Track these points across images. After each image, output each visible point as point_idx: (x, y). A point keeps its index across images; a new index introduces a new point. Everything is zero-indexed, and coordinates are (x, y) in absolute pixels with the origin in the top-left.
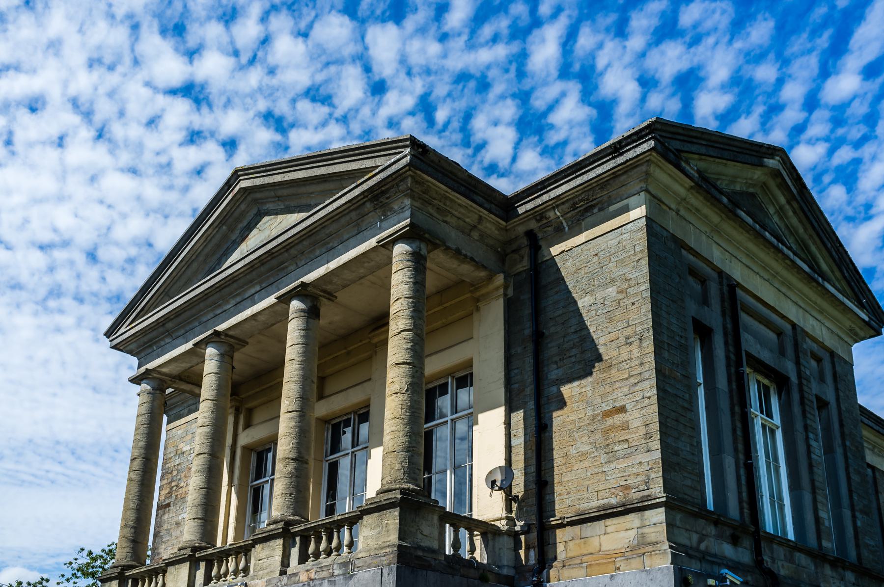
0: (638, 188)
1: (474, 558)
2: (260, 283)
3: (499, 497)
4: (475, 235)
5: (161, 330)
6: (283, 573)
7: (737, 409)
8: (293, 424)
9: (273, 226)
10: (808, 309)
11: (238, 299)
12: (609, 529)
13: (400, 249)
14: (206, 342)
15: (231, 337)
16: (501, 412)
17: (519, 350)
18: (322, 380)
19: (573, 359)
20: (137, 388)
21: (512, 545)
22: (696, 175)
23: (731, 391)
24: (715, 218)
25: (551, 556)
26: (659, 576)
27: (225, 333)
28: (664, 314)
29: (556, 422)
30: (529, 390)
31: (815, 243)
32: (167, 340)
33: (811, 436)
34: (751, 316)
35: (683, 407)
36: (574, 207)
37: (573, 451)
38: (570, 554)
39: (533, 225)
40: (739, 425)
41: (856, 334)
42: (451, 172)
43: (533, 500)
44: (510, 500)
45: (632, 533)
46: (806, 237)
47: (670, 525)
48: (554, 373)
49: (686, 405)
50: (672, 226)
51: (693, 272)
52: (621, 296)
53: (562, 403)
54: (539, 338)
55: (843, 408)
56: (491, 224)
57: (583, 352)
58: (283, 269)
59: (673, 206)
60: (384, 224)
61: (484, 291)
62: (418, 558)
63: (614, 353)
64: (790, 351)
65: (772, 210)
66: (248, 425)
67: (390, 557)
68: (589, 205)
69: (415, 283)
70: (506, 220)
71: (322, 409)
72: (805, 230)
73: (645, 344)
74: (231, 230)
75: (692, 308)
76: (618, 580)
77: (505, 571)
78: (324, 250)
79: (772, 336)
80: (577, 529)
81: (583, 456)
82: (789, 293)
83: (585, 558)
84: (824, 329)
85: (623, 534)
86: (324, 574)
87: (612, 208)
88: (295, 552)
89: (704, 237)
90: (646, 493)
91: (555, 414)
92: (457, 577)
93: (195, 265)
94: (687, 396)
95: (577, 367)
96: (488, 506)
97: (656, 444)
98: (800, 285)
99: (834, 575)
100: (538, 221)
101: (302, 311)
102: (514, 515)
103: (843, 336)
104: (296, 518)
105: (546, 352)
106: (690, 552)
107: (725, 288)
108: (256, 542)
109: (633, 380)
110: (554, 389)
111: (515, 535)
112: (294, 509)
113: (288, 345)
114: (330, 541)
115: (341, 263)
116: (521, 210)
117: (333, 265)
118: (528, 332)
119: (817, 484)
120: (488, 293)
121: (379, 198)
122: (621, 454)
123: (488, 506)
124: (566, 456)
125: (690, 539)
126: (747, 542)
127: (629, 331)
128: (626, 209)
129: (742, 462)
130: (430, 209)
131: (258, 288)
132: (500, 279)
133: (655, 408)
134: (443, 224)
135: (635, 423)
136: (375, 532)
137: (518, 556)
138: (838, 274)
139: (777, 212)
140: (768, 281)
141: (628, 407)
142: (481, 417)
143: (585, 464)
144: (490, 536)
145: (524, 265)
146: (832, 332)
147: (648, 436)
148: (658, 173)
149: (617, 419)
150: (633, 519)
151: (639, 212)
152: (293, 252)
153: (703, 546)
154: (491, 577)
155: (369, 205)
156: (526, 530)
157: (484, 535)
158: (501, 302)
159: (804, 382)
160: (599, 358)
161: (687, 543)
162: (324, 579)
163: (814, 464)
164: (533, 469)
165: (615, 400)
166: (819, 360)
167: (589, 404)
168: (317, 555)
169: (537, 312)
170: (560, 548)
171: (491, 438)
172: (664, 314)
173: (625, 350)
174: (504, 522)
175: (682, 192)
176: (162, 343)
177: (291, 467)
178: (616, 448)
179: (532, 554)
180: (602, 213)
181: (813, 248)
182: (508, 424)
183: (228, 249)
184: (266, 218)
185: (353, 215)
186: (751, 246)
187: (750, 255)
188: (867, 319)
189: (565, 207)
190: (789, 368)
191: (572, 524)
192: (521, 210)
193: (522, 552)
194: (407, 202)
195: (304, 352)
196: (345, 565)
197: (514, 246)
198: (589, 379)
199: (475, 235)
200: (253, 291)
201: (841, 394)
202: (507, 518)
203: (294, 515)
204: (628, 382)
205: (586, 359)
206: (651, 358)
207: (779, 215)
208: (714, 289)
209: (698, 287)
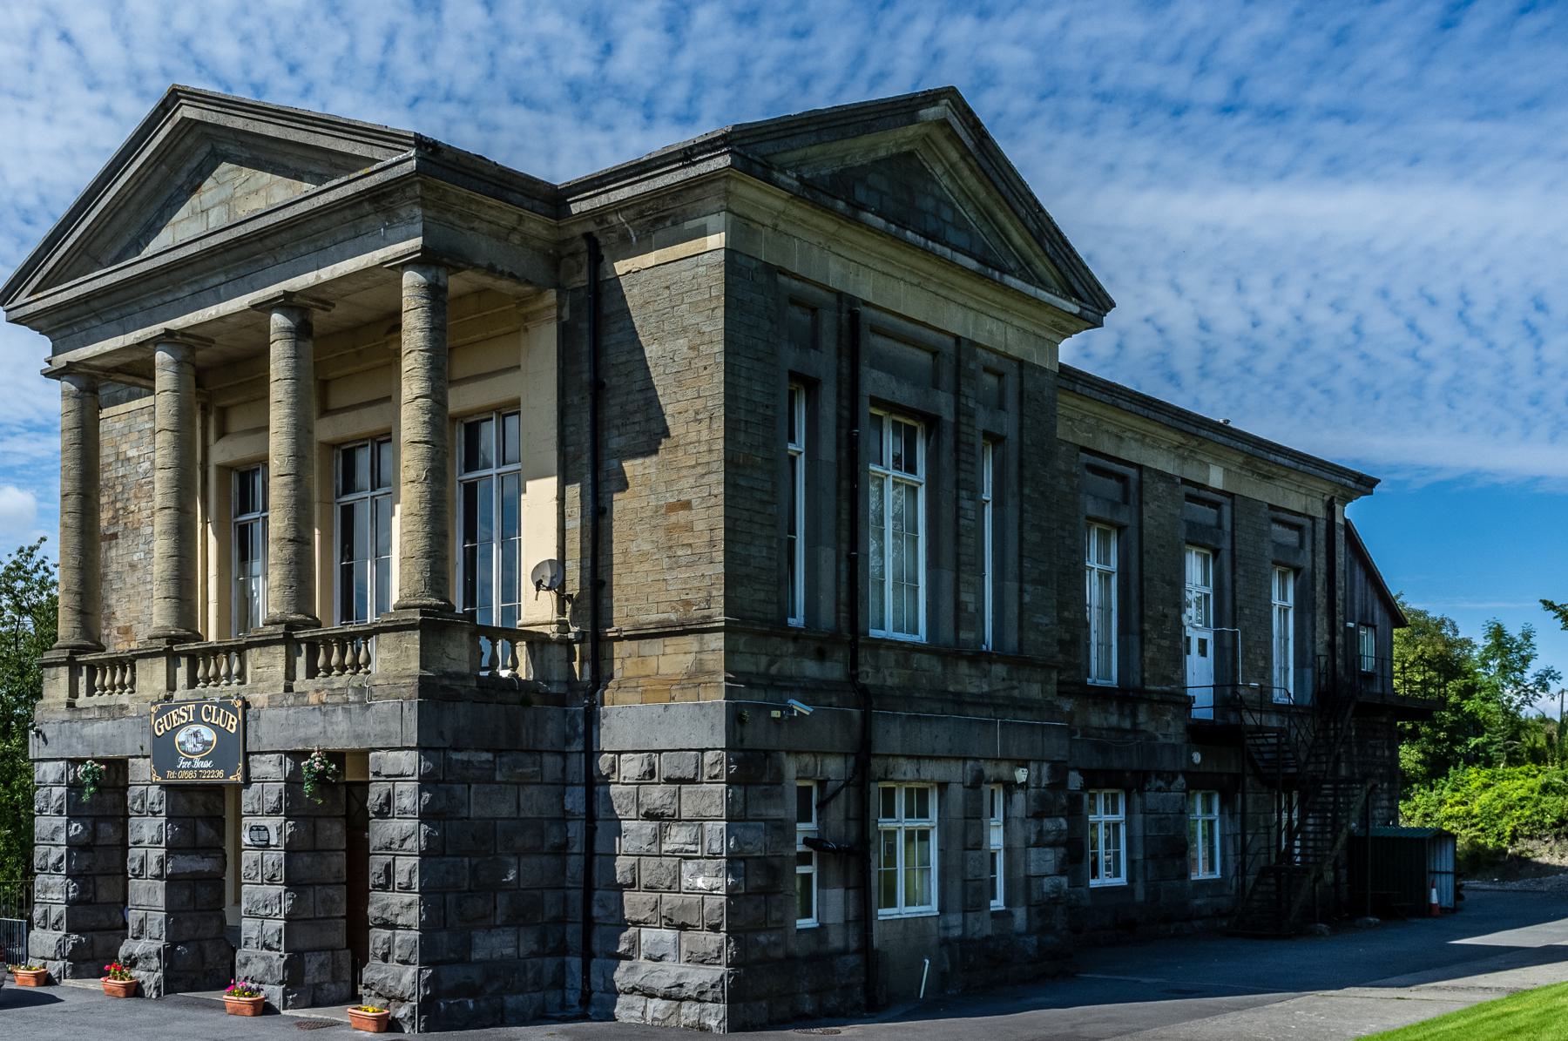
0: (717, 205)
1: (516, 676)
2: (226, 272)
3: (548, 599)
4: (516, 239)
5: (83, 308)
6: (288, 689)
7: (845, 484)
8: (286, 492)
9: (237, 183)
10: (984, 309)
11: (196, 288)
12: (668, 650)
13: (411, 279)
14: (156, 342)
15: (190, 336)
16: (552, 482)
17: (576, 400)
18: (324, 386)
19: (637, 428)
20: (57, 386)
21: (565, 655)
22: (796, 183)
23: (839, 461)
24: (831, 227)
25: (607, 674)
26: (711, 711)
27: (182, 332)
28: (743, 382)
29: (617, 507)
30: (586, 459)
31: (1002, 209)
32: (94, 323)
33: (964, 494)
34: (891, 338)
35: (762, 502)
36: (641, 215)
37: (633, 548)
38: (628, 674)
39: (591, 227)
40: (845, 505)
41: (1062, 329)
42: (475, 170)
43: (587, 602)
44: (562, 599)
45: (691, 658)
46: (990, 203)
47: (730, 652)
48: (615, 442)
49: (765, 498)
50: (765, 252)
51: (795, 301)
52: (692, 354)
53: (624, 486)
54: (598, 388)
55: (1027, 441)
56: (537, 226)
57: (648, 420)
58: (257, 261)
59: (768, 222)
60: (391, 234)
61: (531, 308)
62: (444, 688)
63: (682, 430)
64: (947, 377)
65: (939, 170)
66: (222, 433)
67: (410, 688)
68: (661, 218)
69: (431, 330)
70: (557, 218)
71: (326, 430)
72: (989, 194)
73: (715, 426)
74: (174, 170)
75: (790, 357)
76: (672, 711)
77: (554, 689)
78: (311, 248)
79: (924, 357)
80: (634, 644)
81: (644, 556)
82: (952, 295)
83: (641, 681)
84: (1010, 331)
85: (681, 657)
86: (337, 699)
87: (689, 225)
88: (301, 662)
89: (816, 251)
90: (706, 612)
91: (616, 497)
92: (492, 706)
93: (124, 216)
94: (768, 486)
95: (642, 439)
96: (538, 609)
97: (720, 556)
98: (967, 284)
99: (973, 672)
100: (598, 224)
101: (288, 330)
102: (567, 618)
103: (1042, 333)
104: (300, 617)
105: (604, 424)
106: (754, 680)
107: (845, 316)
108: (250, 645)
109: (700, 470)
110: (615, 462)
111: (570, 643)
112: (296, 605)
113: (272, 378)
114: (343, 655)
115: (337, 274)
116: (575, 209)
117: (326, 274)
118: (586, 377)
119: (963, 558)
120: (538, 311)
121: (380, 203)
122: (683, 561)
123: (538, 609)
124: (625, 553)
125: (757, 664)
126: (841, 654)
127: (699, 404)
128: (702, 232)
129: (844, 554)
130: (450, 216)
131: (223, 278)
132: (551, 296)
133: (721, 510)
134: (469, 233)
135: (700, 526)
136: (392, 655)
137: (572, 667)
138: (1037, 249)
139: (946, 171)
140: (918, 285)
141: (694, 503)
142: (529, 484)
143: (646, 566)
144: (537, 647)
145: (582, 280)
146: (1025, 331)
147: (712, 543)
148: (742, 190)
149: (681, 516)
150: (691, 642)
151: (716, 241)
152: (269, 243)
153: (774, 670)
154: (535, 698)
155: (367, 207)
156: (581, 638)
157: (530, 645)
158: (553, 328)
159: (963, 419)
160: (666, 433)
161: (753, 669)
162: (337, 704)
163: (962, 531)
164: (588, 563)
165: (680, 491)
166: (1000, 375)
167: (653, 492)
168: (329, 670)
169: (597, 353)
170: (617, 664)
171: (541, 515)
172: (743, 382)
173: (694, 427)
174: (554, 627)
175: (778, 204)
176: (87, 325)
177: (289, 550)
178: (680, 553)
179: (587, 667)
180: (675, 229)
181: (1001, 216)
182: (561, 499)
183: (171, 197)
184: (225, 166)
185: (348, 214)
186: (887, 250)
187: (886, 260)
188: (1076, 310)
189: (631, 213)
190: (944, 404)
191: (630, 638)
192: (575, 209)
193: (576, 665)
194: (418, 211)
195: (295, 391)
196: (360, 690)
197: (571, 248)
198: (654, 458)
199: (516, 239)
200: (216, 281)
201: (1027, 421)
202: (558, 622)
203: (297, 613)
204: (694, 471)
205: (652, 435)
206: (720, 445)
207: (950, 175)
208: (828, 322)
209: (807, 319)
